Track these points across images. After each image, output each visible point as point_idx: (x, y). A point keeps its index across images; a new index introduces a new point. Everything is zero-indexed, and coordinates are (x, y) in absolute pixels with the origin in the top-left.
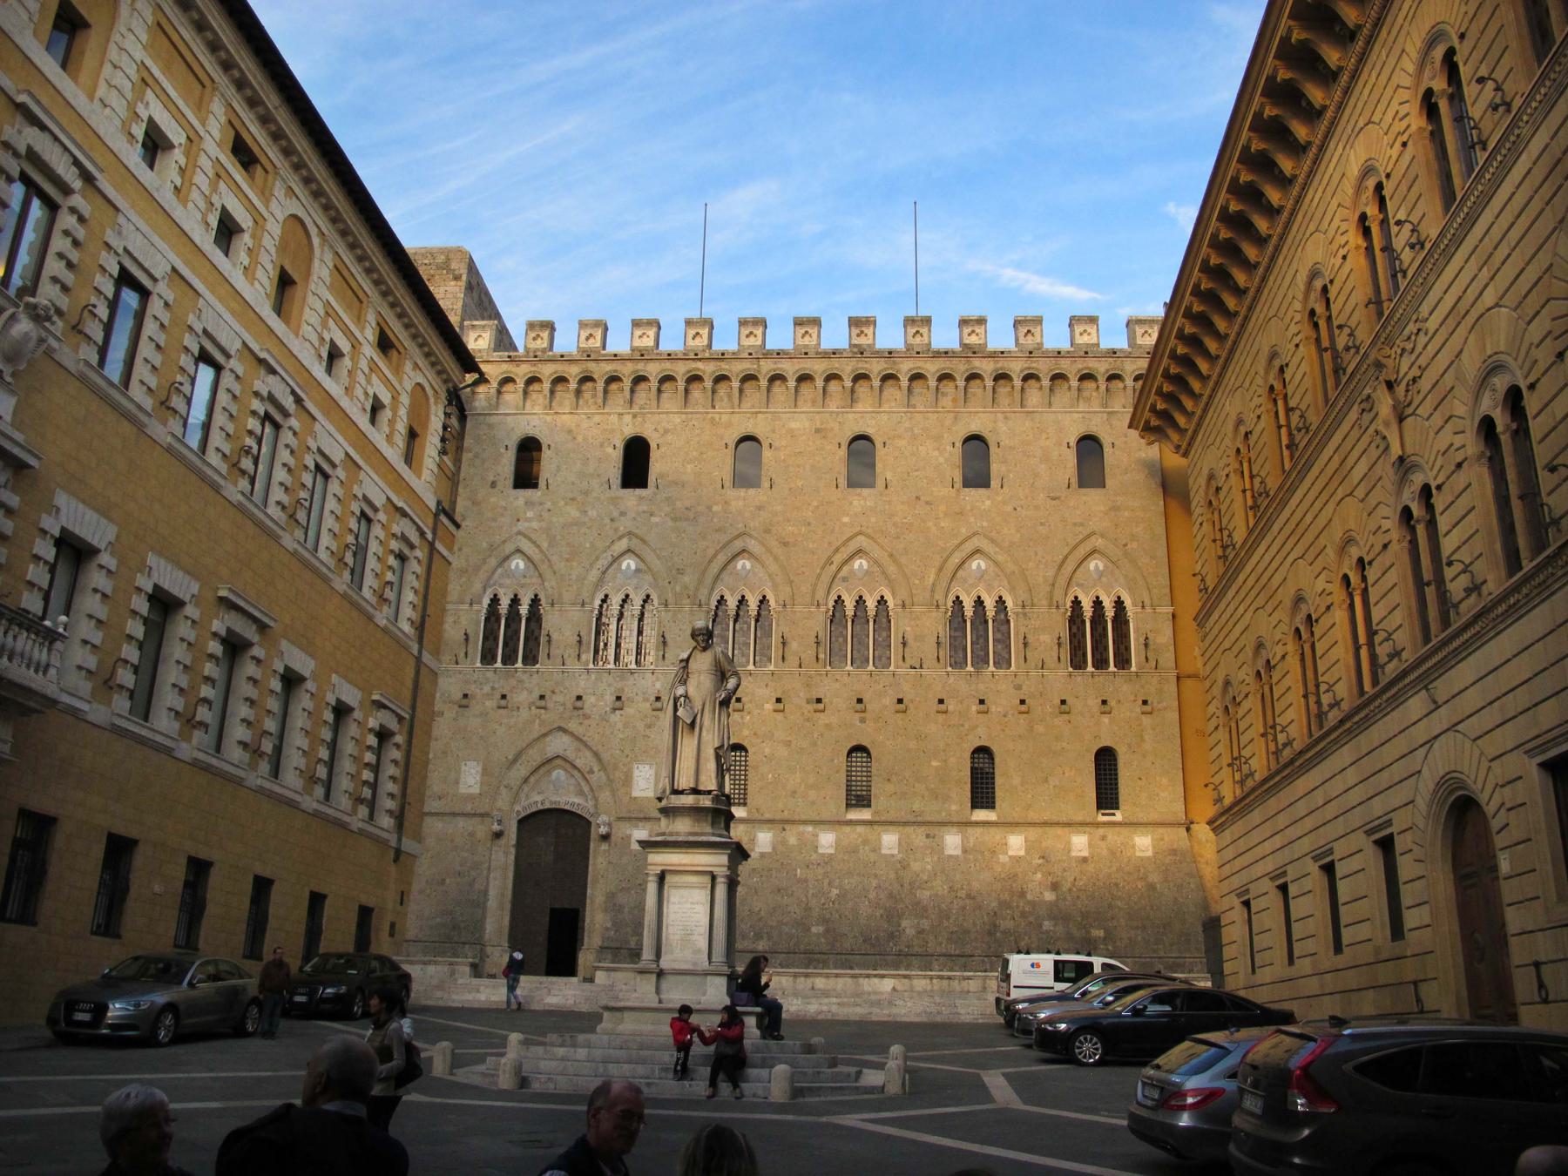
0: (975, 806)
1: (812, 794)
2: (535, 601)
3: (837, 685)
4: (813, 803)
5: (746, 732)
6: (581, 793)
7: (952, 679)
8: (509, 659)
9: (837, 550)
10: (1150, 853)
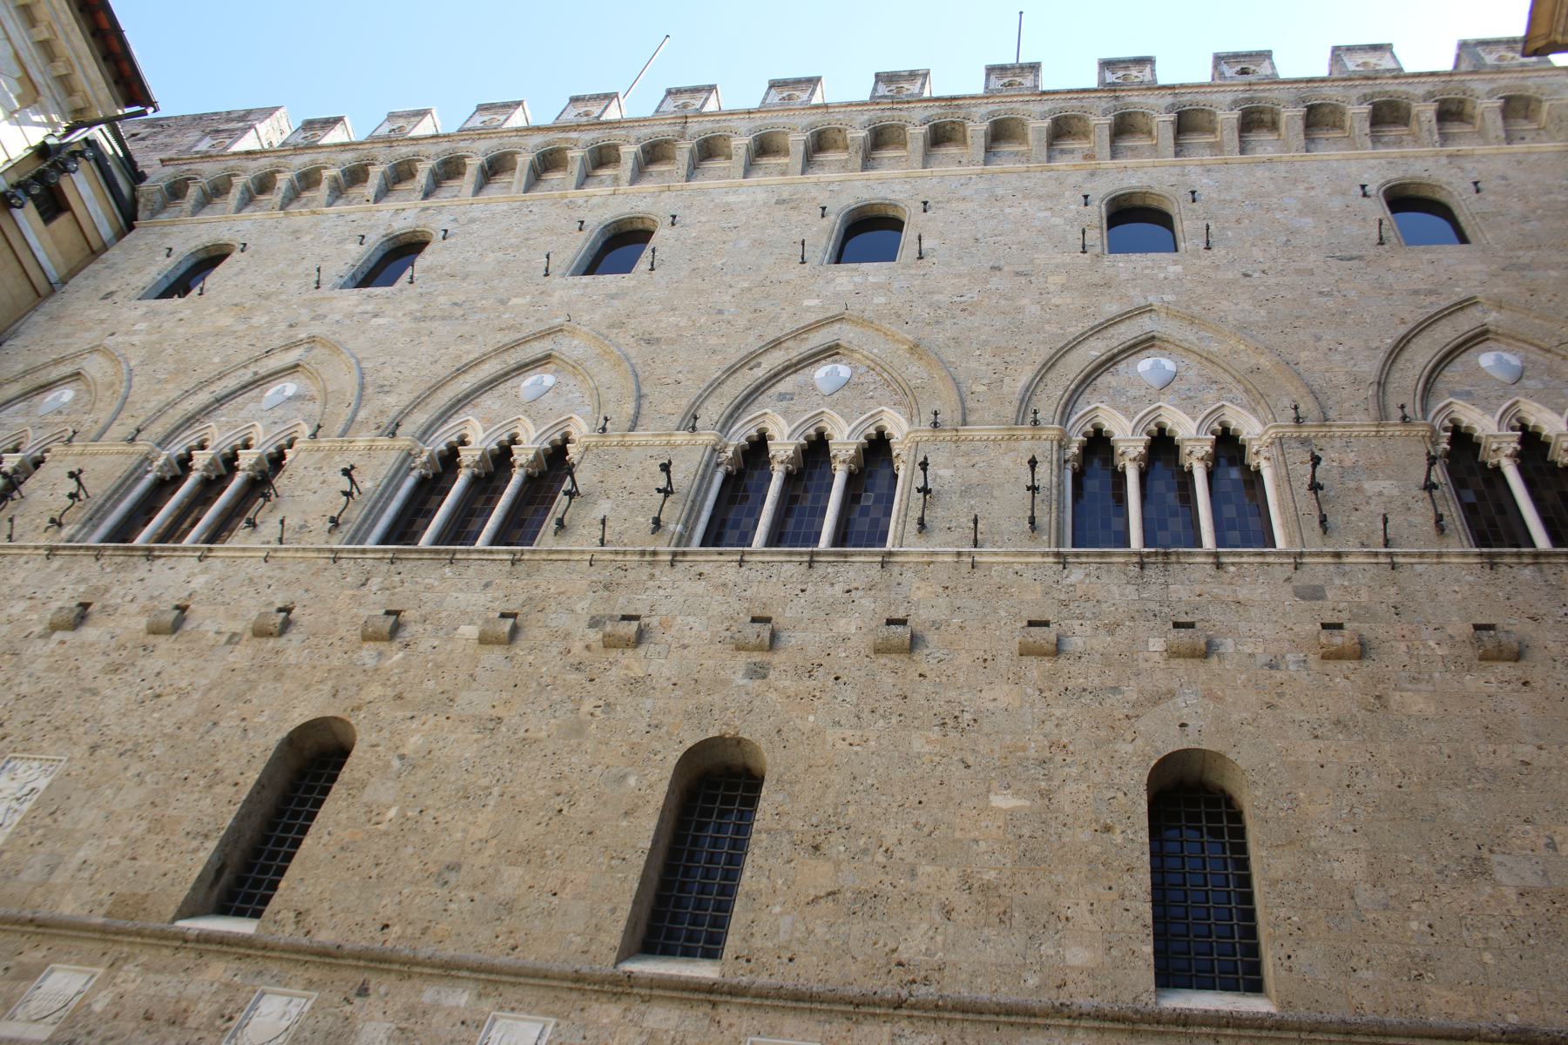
0: (1169, 975)
1: (513, 878)
3: (700, 587)
4: (508, 906)
5: (375, 691)
7: (1076, 575)
9: (776, 344)
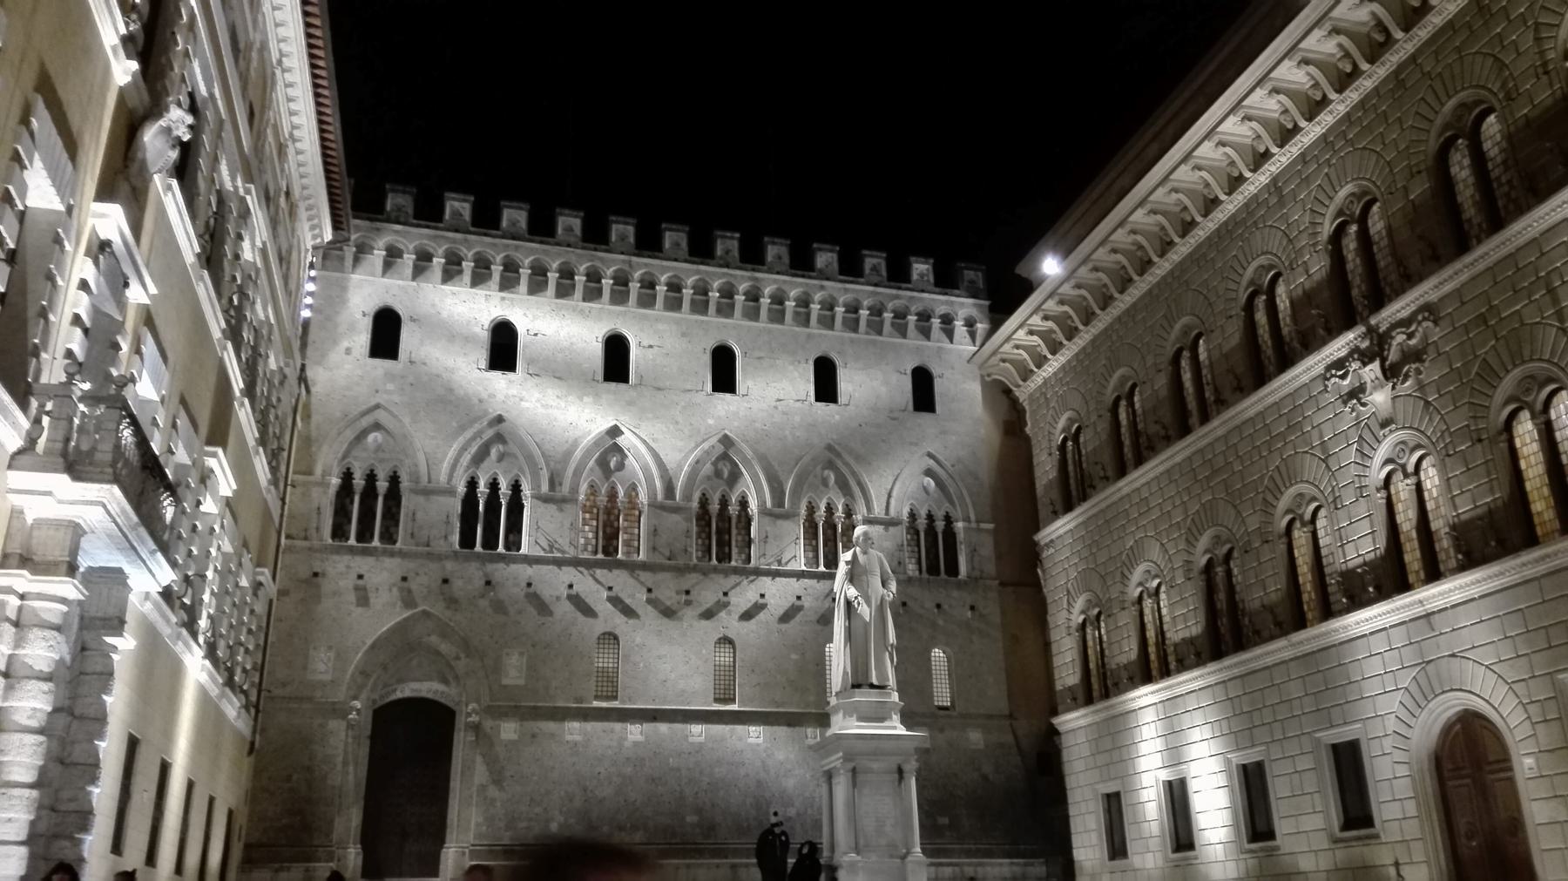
2: (394, 480)
6: (445, 681)
8: (364, 534)
10: (981, 746)
